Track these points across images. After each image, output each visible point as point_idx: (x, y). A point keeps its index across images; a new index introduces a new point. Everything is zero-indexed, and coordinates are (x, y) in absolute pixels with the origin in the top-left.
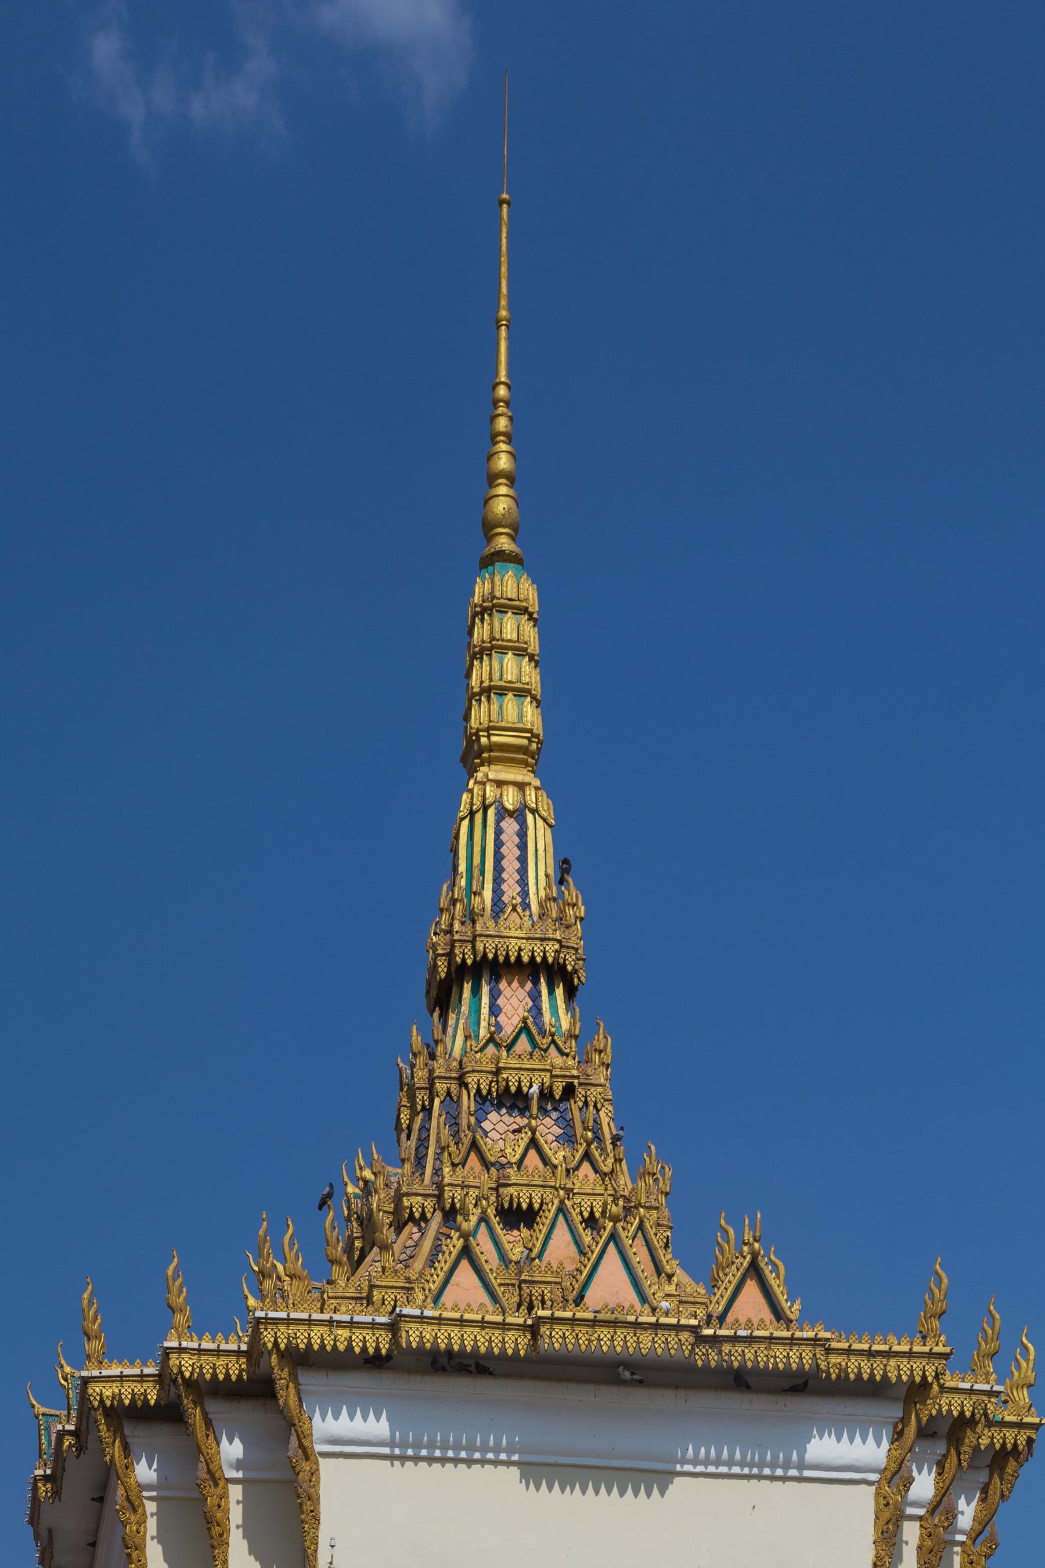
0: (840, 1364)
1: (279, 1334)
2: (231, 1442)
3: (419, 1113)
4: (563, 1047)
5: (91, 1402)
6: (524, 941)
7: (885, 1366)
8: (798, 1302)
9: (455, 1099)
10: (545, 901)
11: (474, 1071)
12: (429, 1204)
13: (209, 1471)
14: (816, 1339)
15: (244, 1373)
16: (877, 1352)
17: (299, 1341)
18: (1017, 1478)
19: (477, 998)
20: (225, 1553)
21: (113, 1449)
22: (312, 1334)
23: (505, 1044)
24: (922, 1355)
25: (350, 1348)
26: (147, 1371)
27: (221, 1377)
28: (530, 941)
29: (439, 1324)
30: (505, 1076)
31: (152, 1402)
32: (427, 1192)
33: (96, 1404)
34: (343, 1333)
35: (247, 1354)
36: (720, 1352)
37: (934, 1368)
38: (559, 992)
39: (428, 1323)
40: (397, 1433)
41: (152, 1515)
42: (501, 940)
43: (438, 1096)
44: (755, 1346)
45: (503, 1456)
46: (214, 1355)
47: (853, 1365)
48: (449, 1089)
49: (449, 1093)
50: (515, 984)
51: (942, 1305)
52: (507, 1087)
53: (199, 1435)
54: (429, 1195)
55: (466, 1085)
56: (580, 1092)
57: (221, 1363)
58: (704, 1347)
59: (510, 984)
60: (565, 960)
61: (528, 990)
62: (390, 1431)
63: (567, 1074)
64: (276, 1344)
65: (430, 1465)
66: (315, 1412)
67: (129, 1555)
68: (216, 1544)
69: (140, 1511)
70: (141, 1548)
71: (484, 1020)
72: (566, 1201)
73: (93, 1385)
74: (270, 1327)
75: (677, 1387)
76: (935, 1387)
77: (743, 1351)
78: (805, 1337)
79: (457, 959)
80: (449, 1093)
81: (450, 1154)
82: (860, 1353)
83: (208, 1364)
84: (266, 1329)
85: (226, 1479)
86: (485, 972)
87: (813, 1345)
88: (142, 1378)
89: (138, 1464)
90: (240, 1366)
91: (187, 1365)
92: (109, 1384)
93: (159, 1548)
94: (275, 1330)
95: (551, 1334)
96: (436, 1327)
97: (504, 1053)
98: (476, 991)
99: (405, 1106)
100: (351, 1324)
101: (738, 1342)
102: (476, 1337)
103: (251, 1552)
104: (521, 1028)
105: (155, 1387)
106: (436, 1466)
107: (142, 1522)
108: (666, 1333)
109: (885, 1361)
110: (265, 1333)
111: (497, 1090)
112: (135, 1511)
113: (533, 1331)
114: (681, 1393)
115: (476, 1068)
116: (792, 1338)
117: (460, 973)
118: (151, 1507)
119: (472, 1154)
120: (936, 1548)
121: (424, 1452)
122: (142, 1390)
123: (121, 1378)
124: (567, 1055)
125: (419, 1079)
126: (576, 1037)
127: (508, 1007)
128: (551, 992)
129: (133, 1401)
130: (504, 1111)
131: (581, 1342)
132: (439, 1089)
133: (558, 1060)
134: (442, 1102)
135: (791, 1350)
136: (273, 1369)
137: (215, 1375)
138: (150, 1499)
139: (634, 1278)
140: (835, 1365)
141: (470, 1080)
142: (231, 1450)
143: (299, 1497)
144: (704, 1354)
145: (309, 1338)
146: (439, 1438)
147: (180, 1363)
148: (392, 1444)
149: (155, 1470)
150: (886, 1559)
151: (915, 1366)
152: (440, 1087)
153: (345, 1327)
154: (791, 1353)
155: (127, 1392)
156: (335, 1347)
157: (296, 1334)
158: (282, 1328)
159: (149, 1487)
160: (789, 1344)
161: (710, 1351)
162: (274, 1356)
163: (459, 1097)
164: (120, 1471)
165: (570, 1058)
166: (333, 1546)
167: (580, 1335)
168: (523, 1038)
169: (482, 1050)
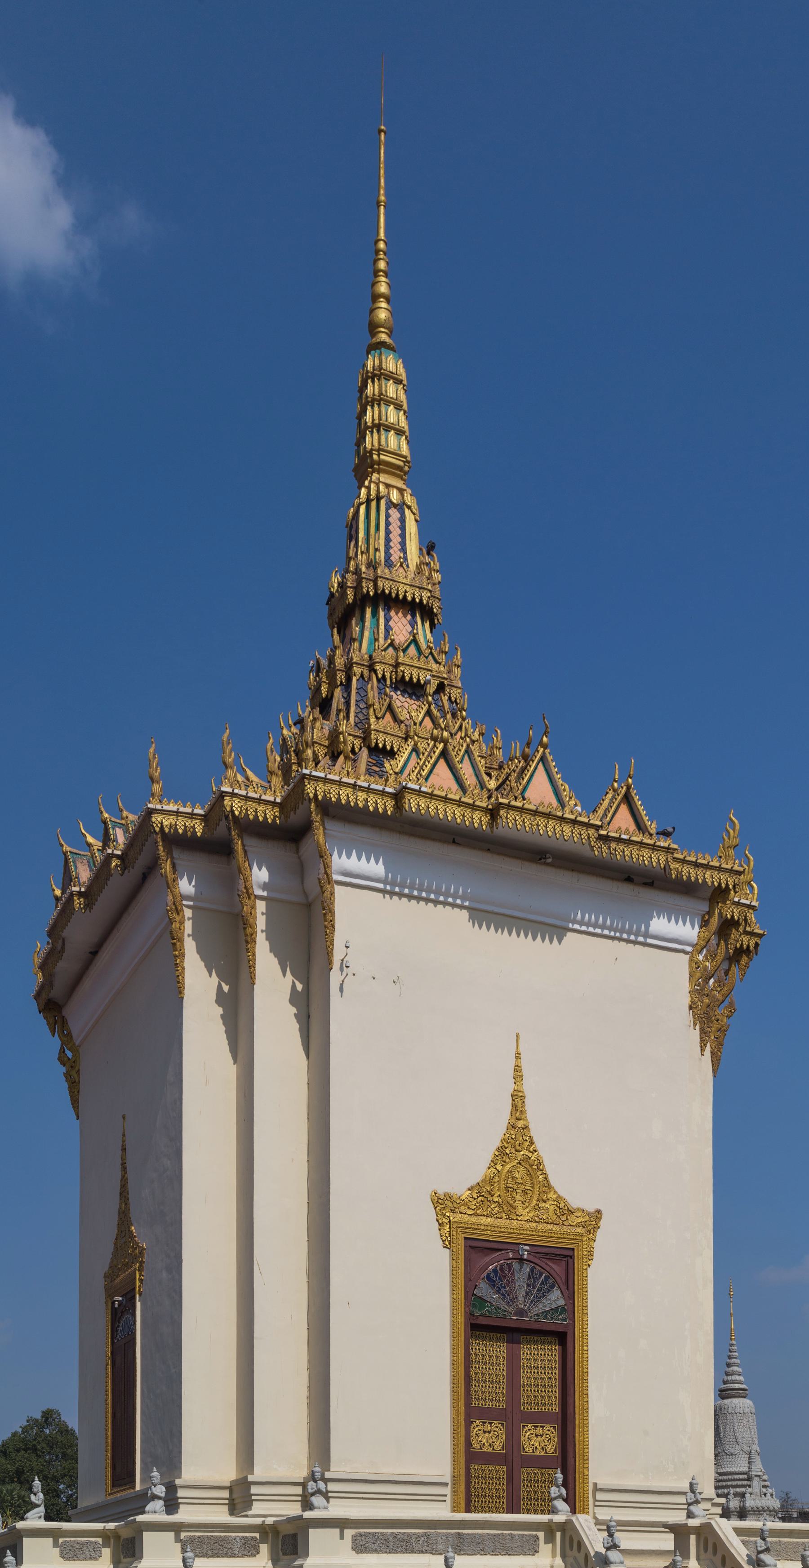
0: (678, 868)
1: (318, 788)
2: (260, 869)
3: (338, 686)
4: (437, 658)
5: (154, 828)
6: (409, 587)
7: (704, 874)
8: (655, 823)
9: (366, 679)
10: (420, 565)
11: (381, 662)
12: (357, 743)
13: (246, 888)
14: (668, 848)
15: (277, 819)
16: (700, 864)
17: (332, 796)
18: (748, 968)
19: (376, 618)
20: (254, 947)
21: (166, 865)
22: (341, 793)
23: (401, 648)
24: (726, 870)
25: (366, 807)
26: (197, 811)
27: (261, 819)
28: (412, 588)
29: (431, 798)
30: (402, 669)
31: (199, 834)
32: (356, 734)
33: (157, 829)
34: (361, 796)
35: (280, 805)
36: (609, 848)
37: (733, 880)
38: (427, 625)
39: (423, 796)
40: (390, 875)
41: (189, 919)
42: (394, 583)
43: (355, 675)
44: (631, 847)
45: (459, 901)
46: (257, 802)
47: (686, 870)
48: (362, 672)
49: (362, 676)
50: (400, 614)
51: (736, 840)
52: (403, 677)
53: (240, 860)
54: (357, 737)
55: (375, 671)
56: (447, 690)
57: (261, 808)
58: (599, 842)
59: (397, 613)
60: (432, 605)
61: (409, 619)
62: (385, 872)
63: (441, 675)
64: (316, 796)
65: (409, 901)
66: (334, 851)
67: (174, 944)
68: (249, 940)
69: (181, 914)
70: (181, 940)
71: (382, 633)
72: (471, 746)
73: (156, 815)
74: (312, 782)
75: (573, 870)
76: (732, 892)
77: (624, 849)
78: (662, 845)
79: (364, 590)
80: (362, 676)
81: (374, 710)
82: (690, 863)
83: (251, 808)
84: (309, 783)
85: (255, 895)
86: (381, 605)
87: (667, 852)
88: (192, 816)
89: (181, 880)
90: (275, 813)
91: (236, 806)
92: (167, 817)
93: (194, 943)
94: (316, 785)
95: (507, 816)
96: (428, 800)
97: (402, 654)
98: (375, 614)
99: (325, 682)
100: (368, 790)
101: (621, 842)
102: (454, 811)
103: (271, 951)
104: (412, 640)
105: (201, 824)
106: (414, 902)
107: (182, 923)
108: (580, 827)
109: (704, 870)
110: (308, 786)
111: (396, 678)
112: (178, 914)
113: (493, 813)
114: (575, 874)
115: (383, 661)
116: (654, 845)
117: (363, 601)
118: (188, 913)
119: (388, 713)
120: (712, 1004)
121: (406, 891)
122: (192, 825)
123: (177, 813)
124: (440, 664)
125: (339, 664)
126: (446, 653)
127: (396, 627)
128: (423, 624)
129: (185, 831)
130: (399, 693)
131: (526, 825)
132: (356, 671)
133: (435, 666)
134: (358, 680)
135: (653, 853)
136: (312, 813)
137: (256, 816)
138: (188, 907)
139: (555, 789)
140: (675, 868)
141: (378, 668)
142: (260, 875)
143: (324, 909)
144: (599, 847)
145: (339, 795)
146: (417, 882)
147: (232, 804)
148: (385, 882)
149: (193, 886)
150: (699, 1003)
151: (722, 877)
152: (357, 670)
153: (363, 791)
154: (653, 856)
155: (181, 824)
156: (356, 804)
157: (330, 790)
158: (321, 785)
159: (188, 898)
160: (652, 849)
161: (603, 846)
162: (313, 804)
163: (370, 678)
164: (170, 882)
165: (442, 666)
166: (347, 947)
167: (526, 820)
168: (412, 647)
169: (385, 650)
